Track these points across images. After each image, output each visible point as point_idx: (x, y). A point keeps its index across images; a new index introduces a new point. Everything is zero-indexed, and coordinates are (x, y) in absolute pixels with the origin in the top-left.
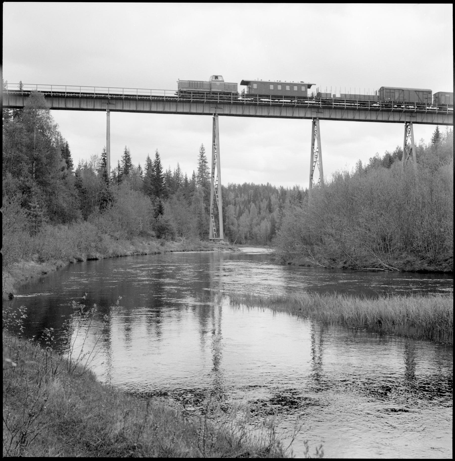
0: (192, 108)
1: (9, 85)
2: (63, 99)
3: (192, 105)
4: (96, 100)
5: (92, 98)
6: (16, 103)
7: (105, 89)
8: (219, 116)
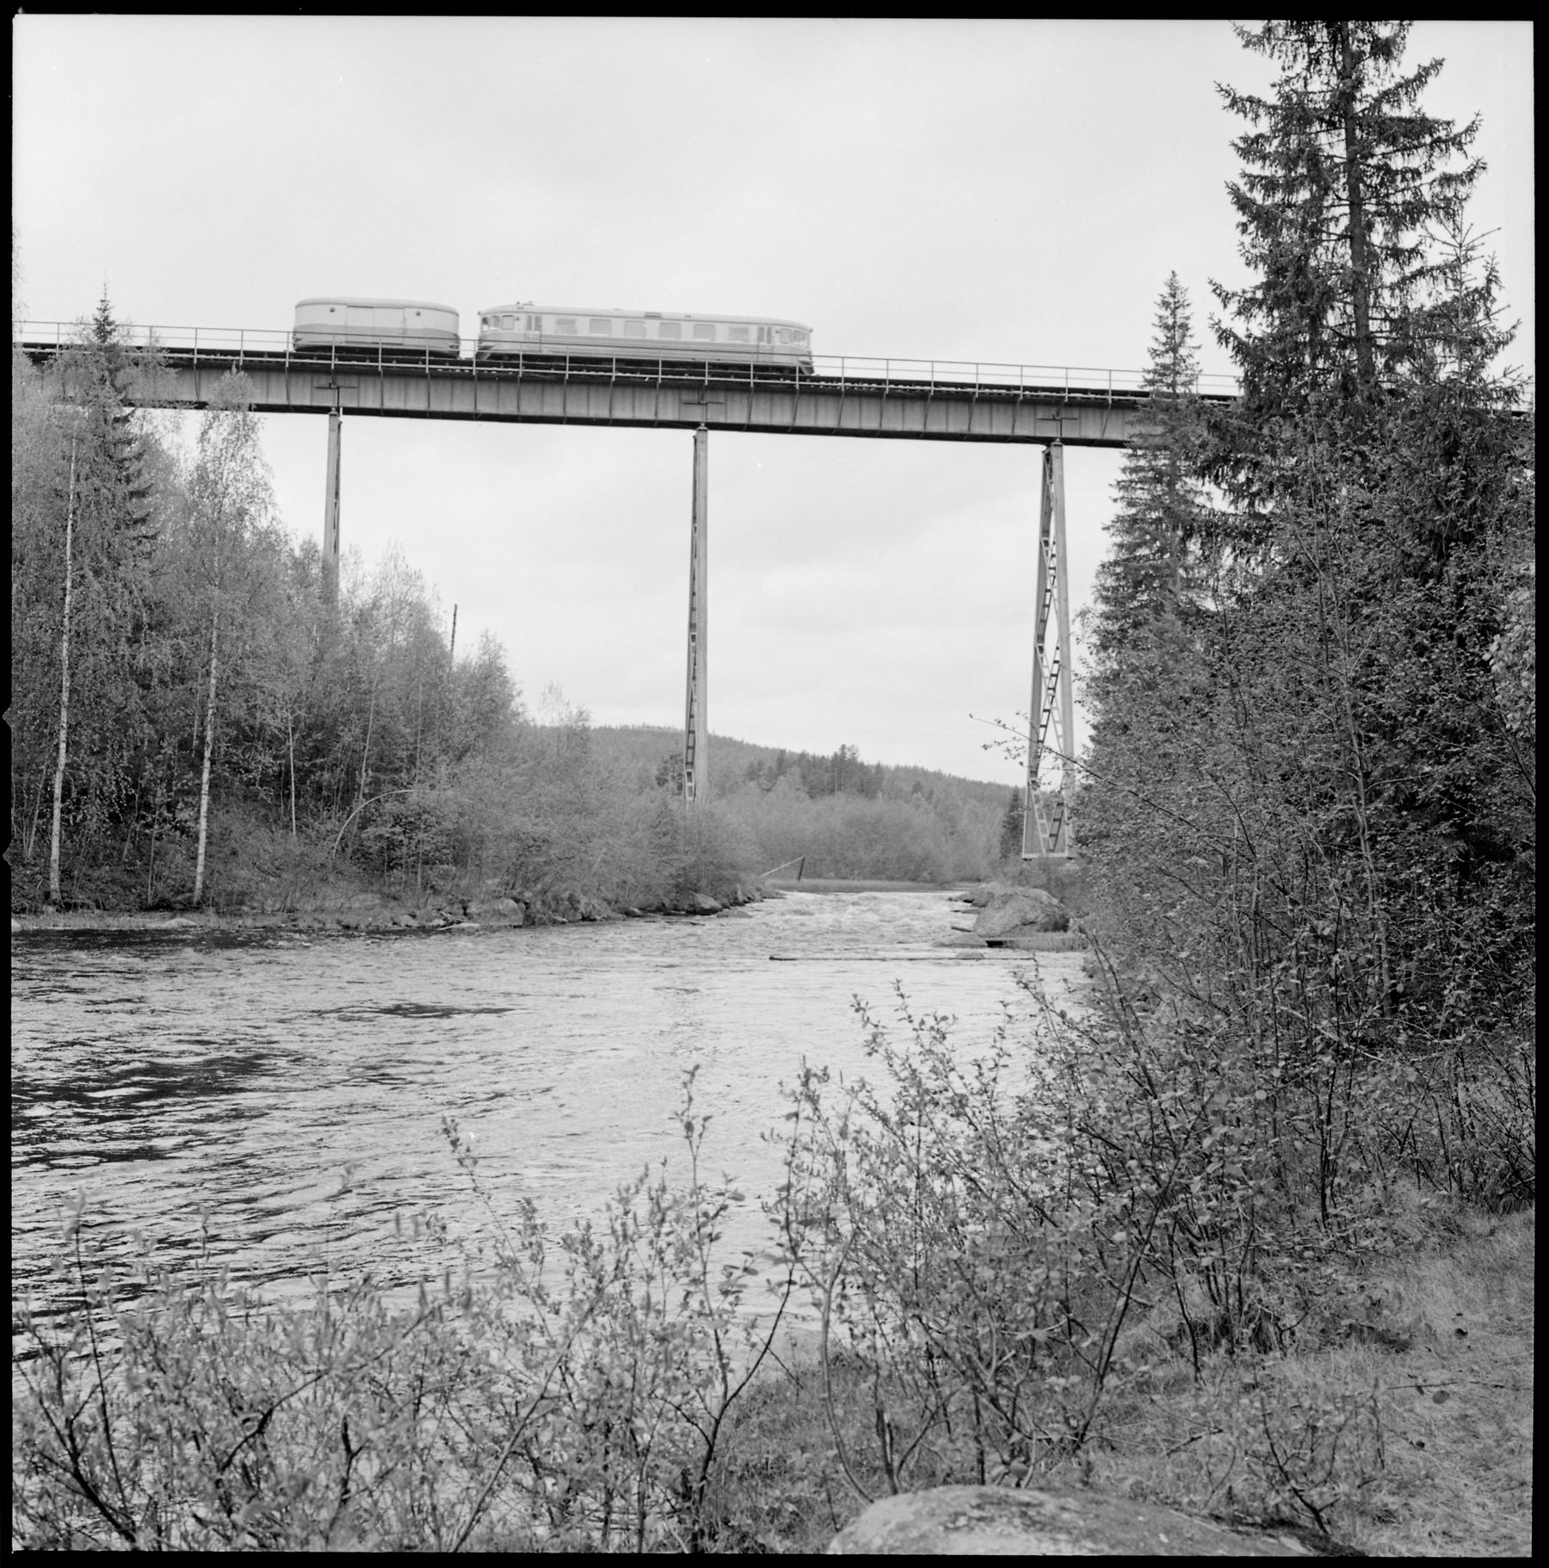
0: (976, 416)
1: (1201, 379)
2: (468, 386)
3: (977, 410)
4: (618, 393)
5: (922, 397)
6: (405, 402)
7: (965, 368)
8: (1066, 449)
